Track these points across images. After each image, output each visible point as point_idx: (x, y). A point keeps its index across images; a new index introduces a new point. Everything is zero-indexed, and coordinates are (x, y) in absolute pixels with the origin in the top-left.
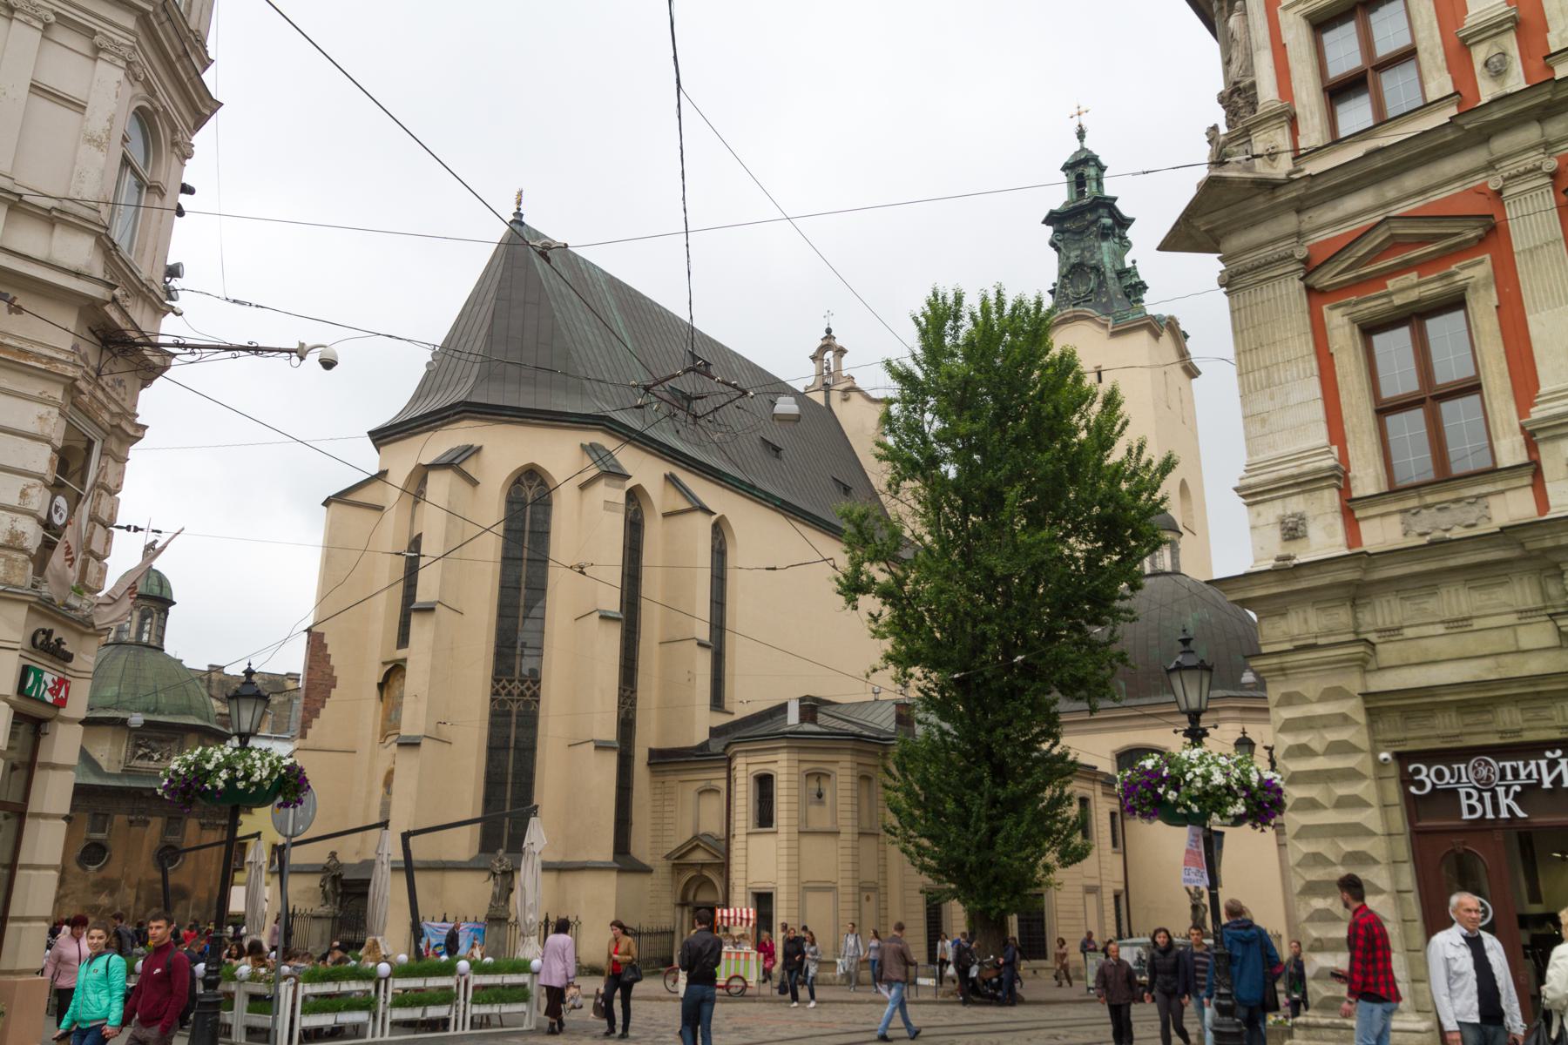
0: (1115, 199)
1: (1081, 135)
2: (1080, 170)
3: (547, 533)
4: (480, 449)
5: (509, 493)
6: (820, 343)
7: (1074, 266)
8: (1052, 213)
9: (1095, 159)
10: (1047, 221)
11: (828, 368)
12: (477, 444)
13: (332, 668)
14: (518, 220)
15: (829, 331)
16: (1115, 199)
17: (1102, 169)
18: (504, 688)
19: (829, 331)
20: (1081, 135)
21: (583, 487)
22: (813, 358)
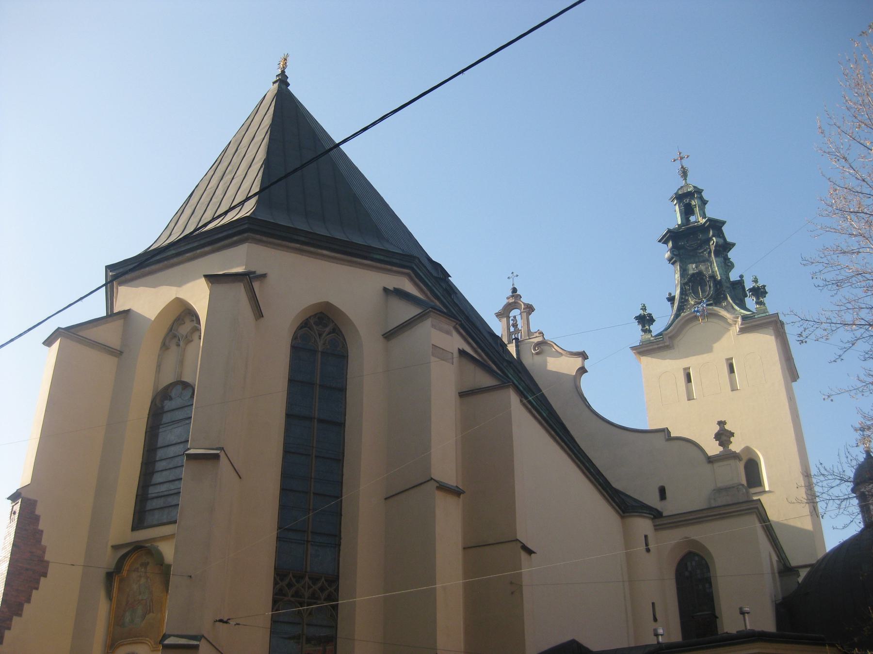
0: (724, 223)
1: (684, 173)
2: (687, 201)
3: (343, 390)
4: (264, 276)
5: (295, 338)
6: (505, 302)
7: (693, 275)
8: (669, 231)
9: (699, 191)
10: (664, 240)
11: (515, 325)
12: (260, 272)
13: (44, 550)
14: (282, 80)
15: (514, 290)
16: (724, 223)
17: (704, 202)
18: (290, 585)
19: (514, 290)
20: (684, 173)
21: (389, 336)
22: (499, 315)
